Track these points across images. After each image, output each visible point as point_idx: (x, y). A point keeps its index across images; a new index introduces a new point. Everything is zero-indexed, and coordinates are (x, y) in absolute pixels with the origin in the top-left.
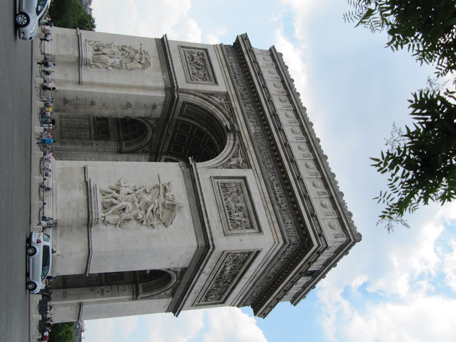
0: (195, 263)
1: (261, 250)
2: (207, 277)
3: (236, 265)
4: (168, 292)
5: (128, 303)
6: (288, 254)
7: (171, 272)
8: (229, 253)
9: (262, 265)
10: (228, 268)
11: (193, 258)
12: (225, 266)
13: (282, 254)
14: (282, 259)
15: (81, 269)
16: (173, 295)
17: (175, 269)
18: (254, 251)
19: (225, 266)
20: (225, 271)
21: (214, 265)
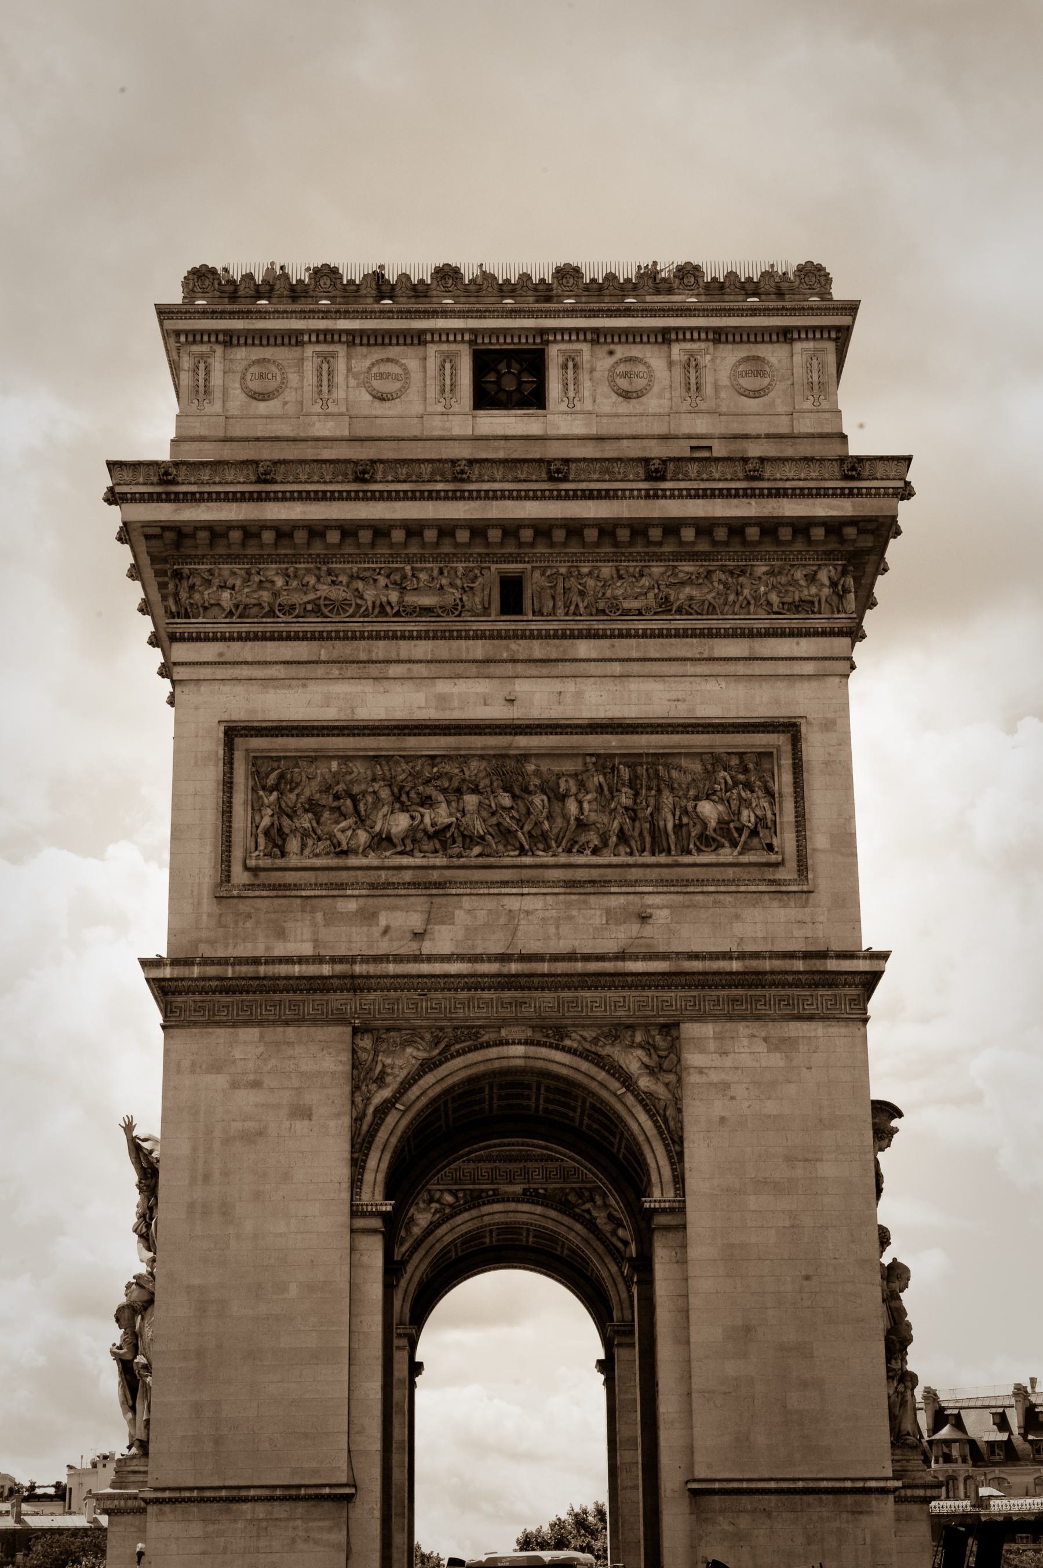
0: (311, 1003)
1: (222, 729)
2: (466, 903)
3: (385, 794)
4: (633, 1061)
5: (696, 1251)
6: (280, 582)
7: (415, 1091)
8: (246, 868)
9: (374, 670)
10: (401, 822)
11: (260, 1023)
12: (382, 841)
13: (271, 613)
14: (311, 596)
15: (299, 1523)
16: (670, 1028)
17: (389, 1079)
18: (247, 750)
19: (382, 841)
20: (425, 831)
21: (352, 905)
